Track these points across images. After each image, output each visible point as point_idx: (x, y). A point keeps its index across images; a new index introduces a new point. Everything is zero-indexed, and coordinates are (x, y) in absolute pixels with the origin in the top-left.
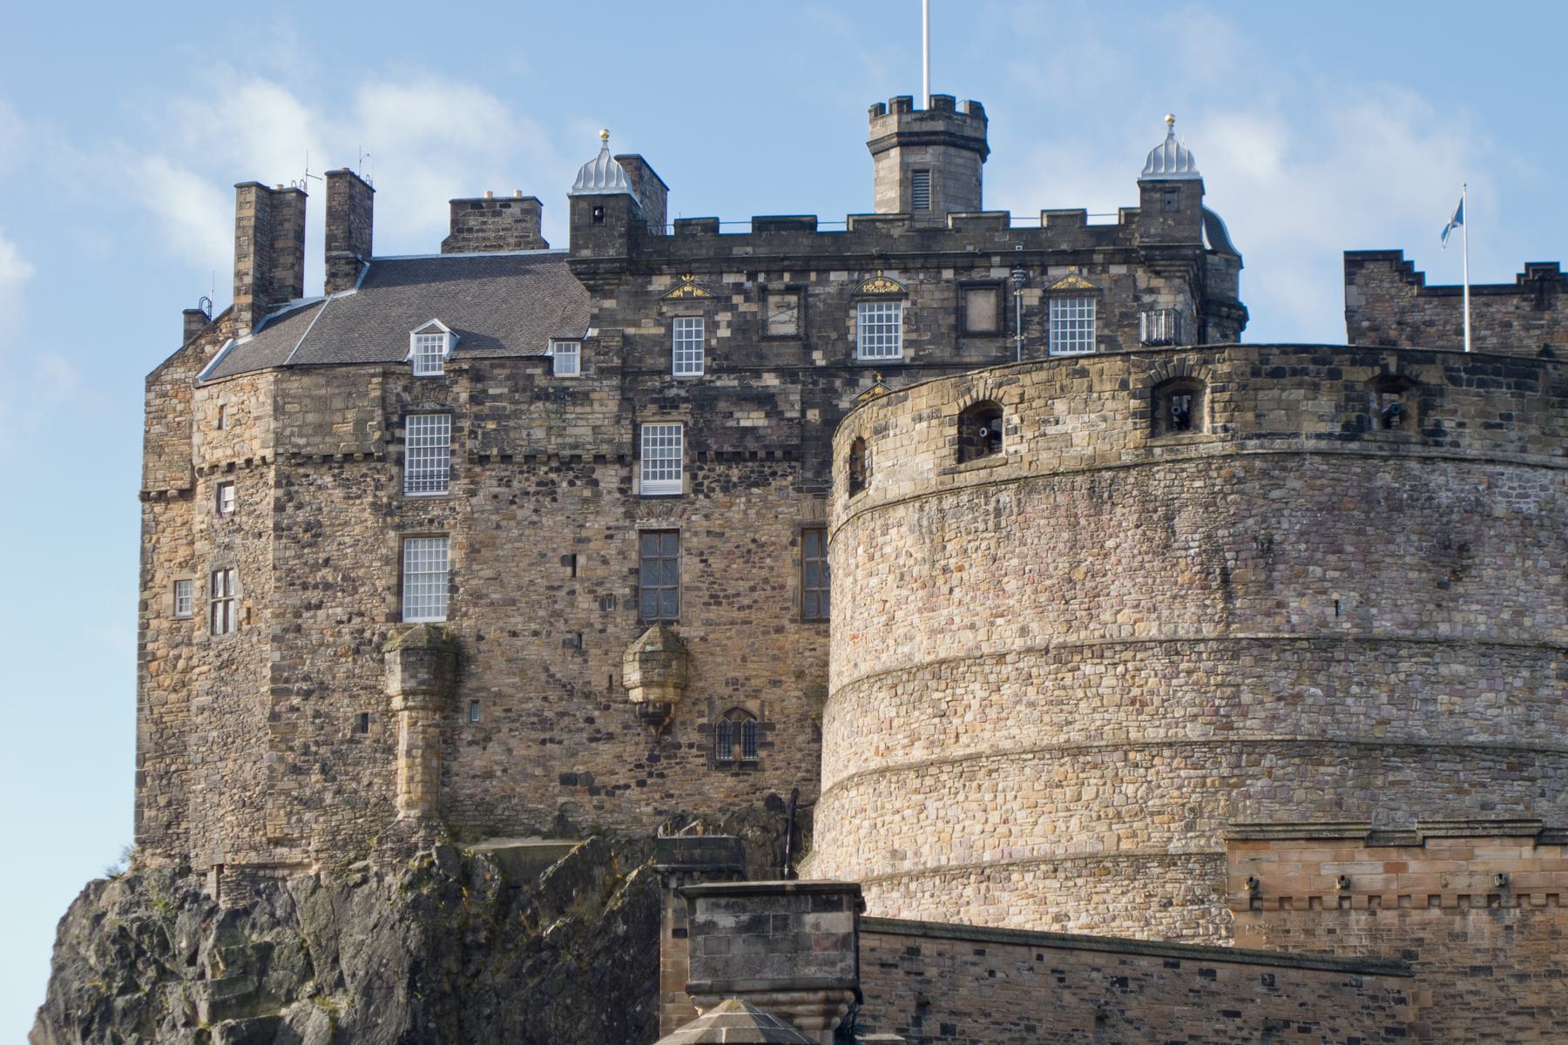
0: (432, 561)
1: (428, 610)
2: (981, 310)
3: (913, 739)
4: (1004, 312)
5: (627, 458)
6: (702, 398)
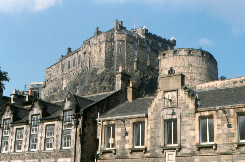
2: (165, 45)
3: (185, 71)
4: (166, 45)
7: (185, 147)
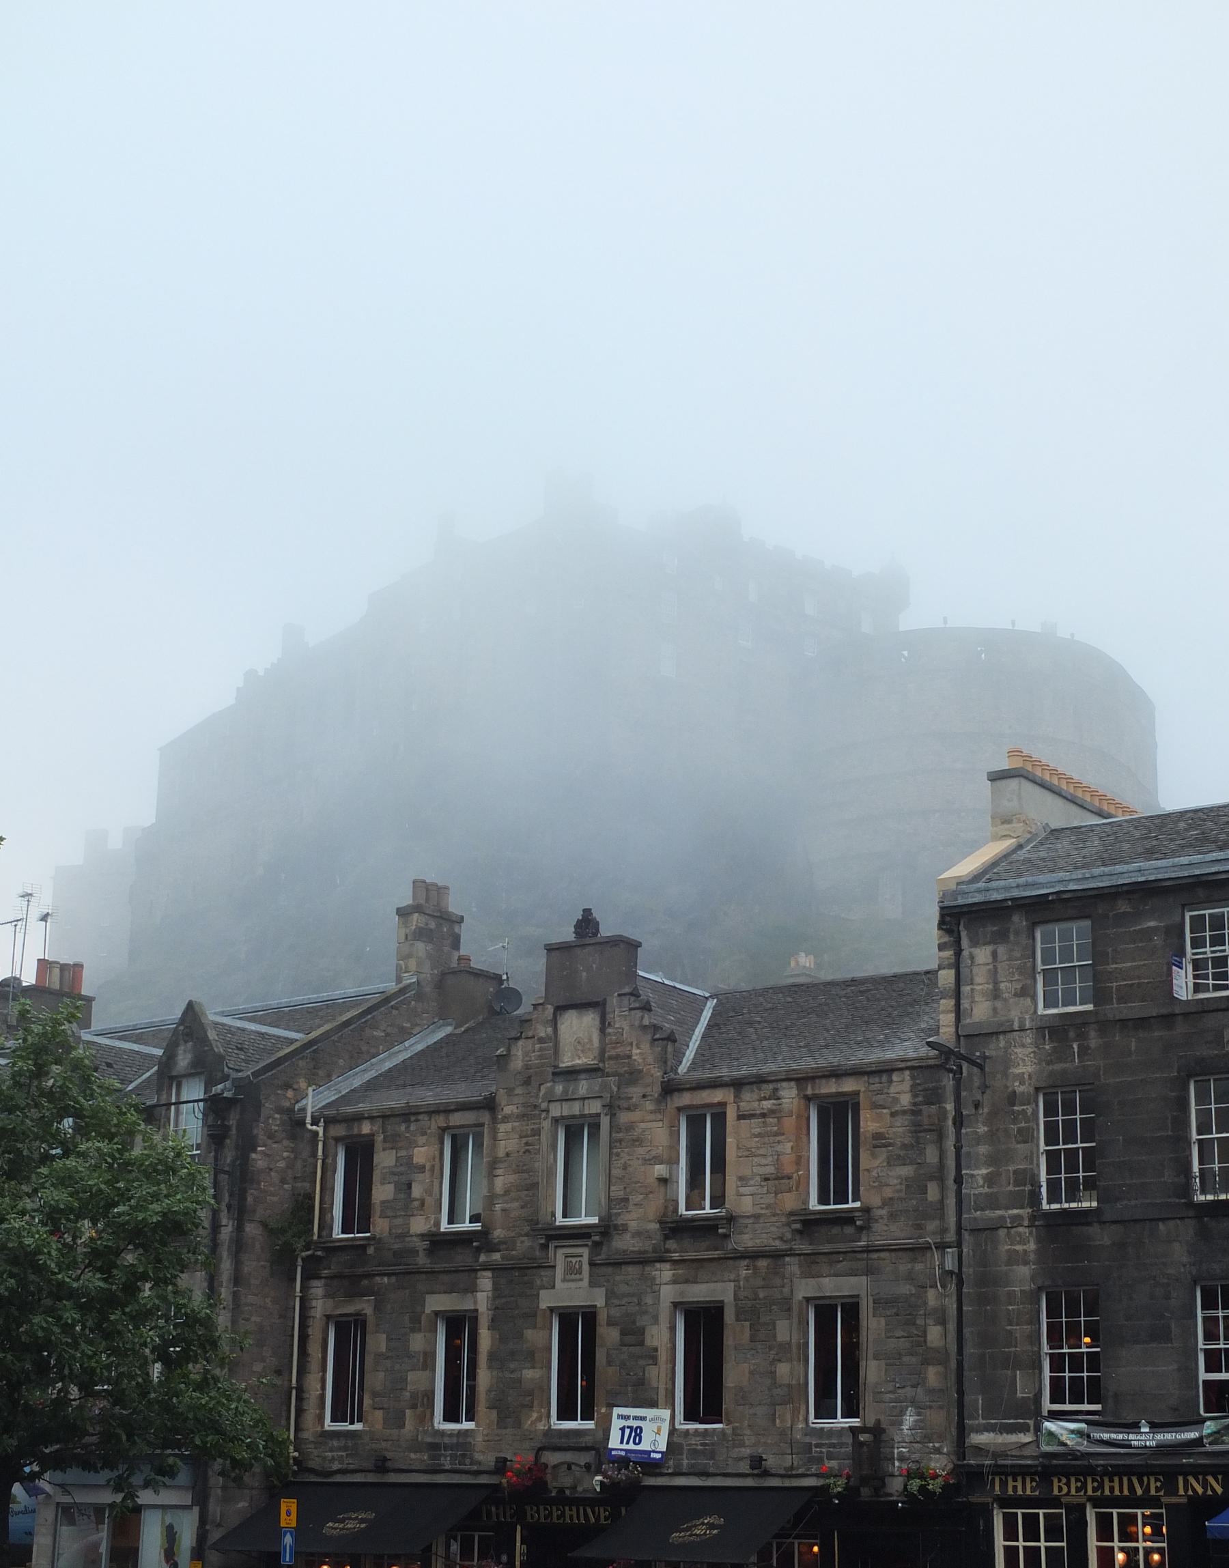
7: (625, 1228)
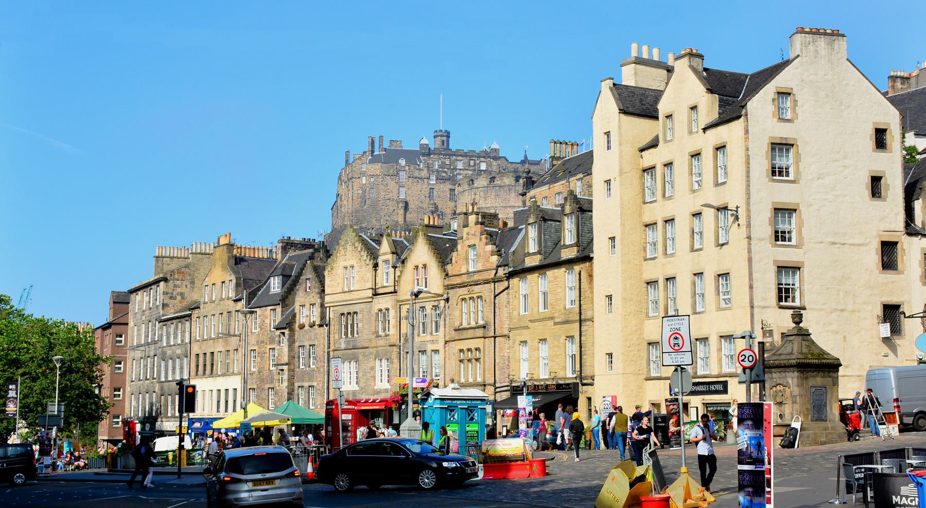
0: (403, 190)
1: (402, 197)
2: (472, 163)
5: (428, 178)
6: (438, 171)
